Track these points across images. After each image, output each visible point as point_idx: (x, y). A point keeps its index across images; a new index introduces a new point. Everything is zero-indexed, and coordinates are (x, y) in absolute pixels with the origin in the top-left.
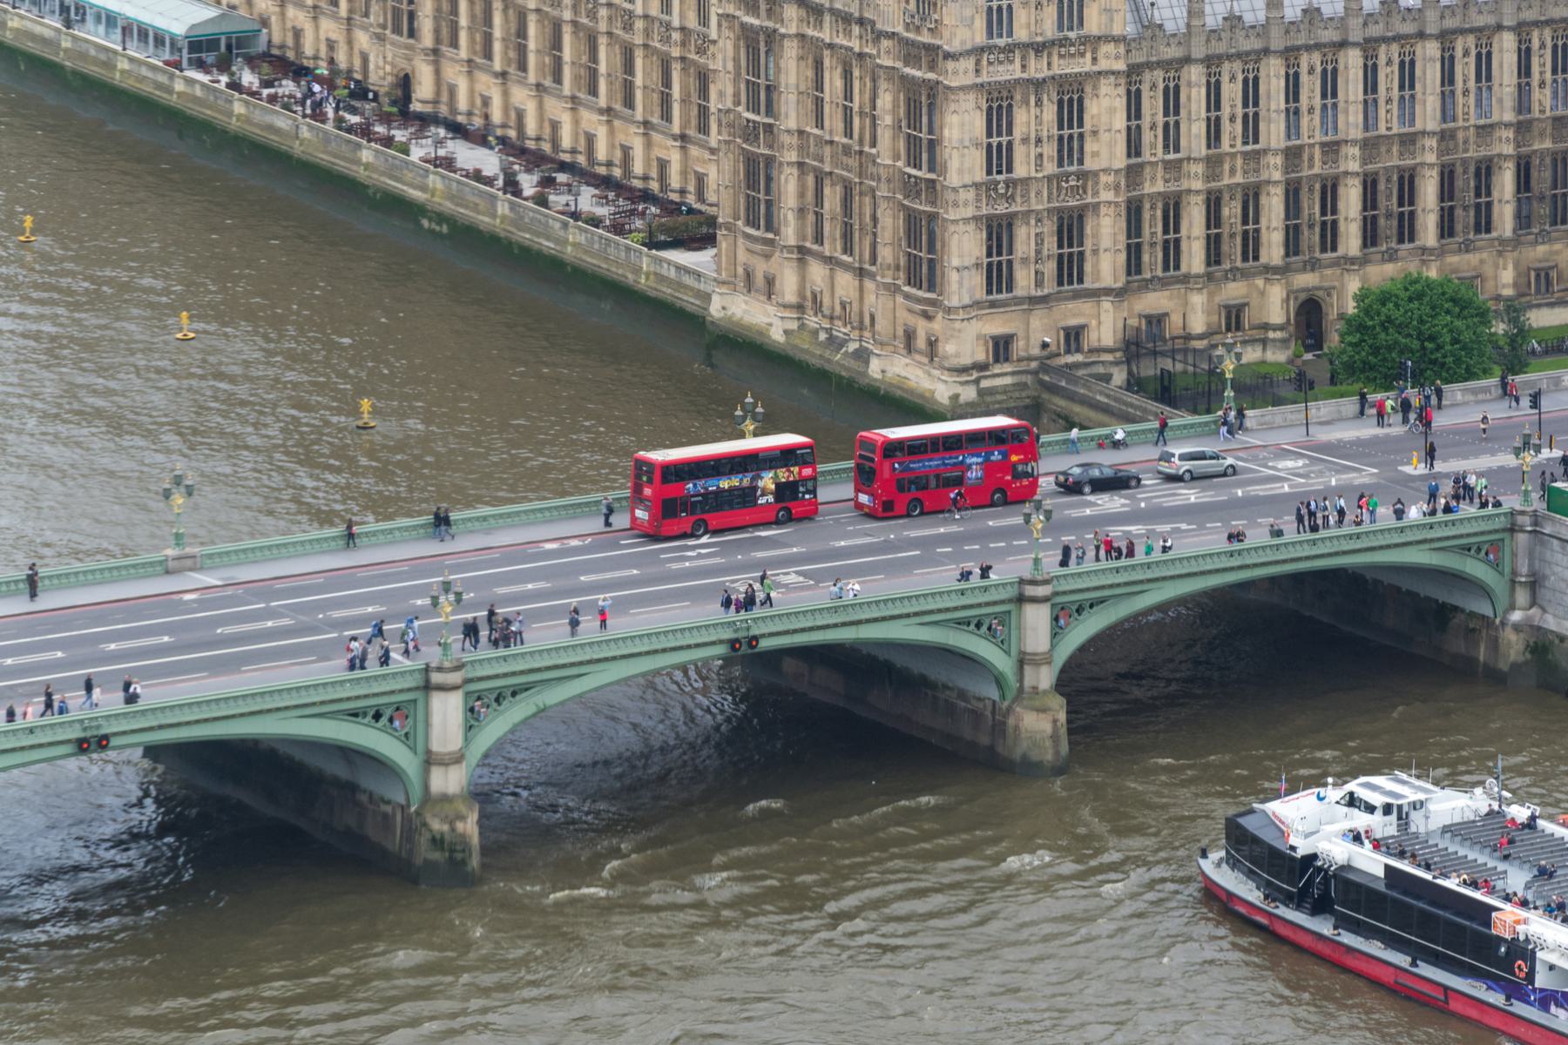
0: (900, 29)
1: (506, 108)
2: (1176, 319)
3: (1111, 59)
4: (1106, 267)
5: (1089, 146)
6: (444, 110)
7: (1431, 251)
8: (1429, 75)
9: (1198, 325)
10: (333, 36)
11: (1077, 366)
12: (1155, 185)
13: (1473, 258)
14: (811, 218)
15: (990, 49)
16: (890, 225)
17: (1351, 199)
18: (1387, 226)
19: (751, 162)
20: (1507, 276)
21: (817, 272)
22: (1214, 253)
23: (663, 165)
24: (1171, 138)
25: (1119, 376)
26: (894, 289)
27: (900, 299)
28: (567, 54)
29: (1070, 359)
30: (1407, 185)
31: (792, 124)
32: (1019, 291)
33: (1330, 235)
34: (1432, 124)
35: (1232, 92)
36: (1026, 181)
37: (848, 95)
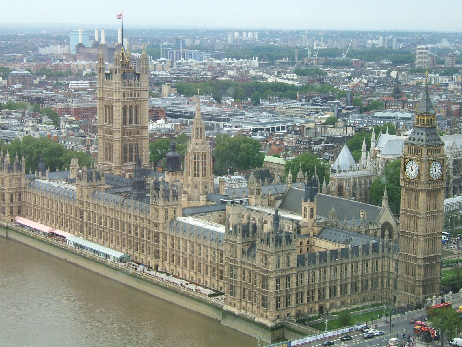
0: (261, 267)
1: (176, 271)
2: (303, 311)
3: (294, 271)
4: (293, 303)
5: (291, 285)
6: (164, 271)
7: (339, 298)
8: (339, 270)
9: (306, 311)
10: (143, 258)
11: (289, 319)
12: (300, 290)
13: (344, 298)
14: (242, 295)
15: (277, 270)
16: (259, 298)
17: (328, 291)
18: (333, 294)
19: (231, 285)
20: (349, 301)
21: (244, 304)
22: (308, 301)
23: (206, 282)
24: (302, 282)
25: (295, 320)
26: (259, 307)
27: (261, 309)
28: (188, 263)
29: (288, 318)
30: (335, 288)
31: (239, 280)
32: (281, 308)
33: (324, 296)
34: (339, 278)
35: (311, 275)
36: (282, 291)
37: (250, 275)
